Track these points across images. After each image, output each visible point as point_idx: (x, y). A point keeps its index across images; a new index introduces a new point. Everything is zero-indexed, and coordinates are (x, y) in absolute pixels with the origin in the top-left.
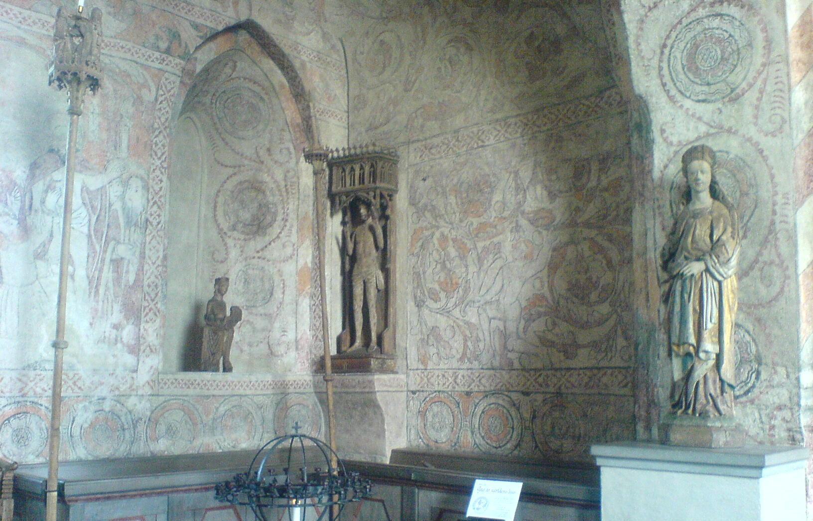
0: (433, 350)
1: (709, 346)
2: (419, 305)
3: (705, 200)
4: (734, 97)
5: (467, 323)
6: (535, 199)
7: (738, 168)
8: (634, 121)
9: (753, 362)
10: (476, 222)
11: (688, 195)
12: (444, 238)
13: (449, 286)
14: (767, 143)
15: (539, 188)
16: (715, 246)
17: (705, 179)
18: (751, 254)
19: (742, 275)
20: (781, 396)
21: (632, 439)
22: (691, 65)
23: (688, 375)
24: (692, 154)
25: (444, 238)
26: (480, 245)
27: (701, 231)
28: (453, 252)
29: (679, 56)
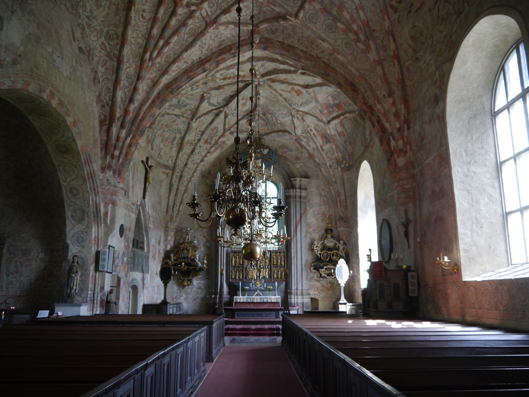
0: (10, 286)
1: (75, 288)
2: (7, 275)
3: (76, 264)
4: (83, 247)
5: (21, 281)
6: (42, 255)
7: (82, 258)
8: (66, 247)
9: (81, 290)
10: (26, 258)
11: (73, 262)
12: (17, 261)
13: (17, 272)
14: (87, 255)
15: (43, 254)
16: (77, 272)
17: (76, 260)
18: (83, 272)
19: (80, 277)
20: (85, 295)
21: (59, 302)
22: (77, 240)
23: (71, 291)
24: (75, 256)
25: (17, 261)
26: (27, 263)
27: (75, 269)
28: (19, 264)
29: (75, 238)
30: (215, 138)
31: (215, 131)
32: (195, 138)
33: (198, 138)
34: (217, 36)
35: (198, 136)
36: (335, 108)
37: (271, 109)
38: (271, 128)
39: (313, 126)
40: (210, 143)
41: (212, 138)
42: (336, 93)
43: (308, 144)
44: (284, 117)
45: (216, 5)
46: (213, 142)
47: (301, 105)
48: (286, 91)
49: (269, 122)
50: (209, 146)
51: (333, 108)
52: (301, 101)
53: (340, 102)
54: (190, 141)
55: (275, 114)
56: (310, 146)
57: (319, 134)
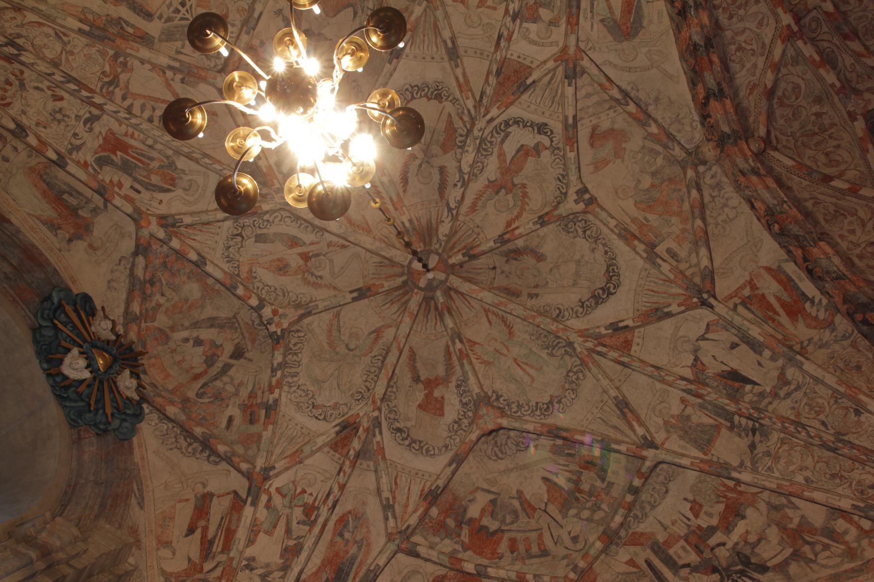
30: (127, 182)
31: (155, 179)
32: (136, 96)
33: (136, 110)
34: (740, 49)
35: (143, 108)
36: (465, 532)
37: (305, 357)
38: (191, 394)
39: (349, 507)
40: (102, 162)
41: (126, 168)
42: (516, 503)
43: (254, 531)
44: (298, 405)
45: (814, 35)
46: (108, 175)
47: (399, 430)
48: (414, 369)
49: (216, 378)
50: (90, 159)
51: (459, 526)
52: (409, 424)
53: (500, 531)
54: (123, 77)
55: (294, 375)
56: (250, 542)
57: (332, 543)
